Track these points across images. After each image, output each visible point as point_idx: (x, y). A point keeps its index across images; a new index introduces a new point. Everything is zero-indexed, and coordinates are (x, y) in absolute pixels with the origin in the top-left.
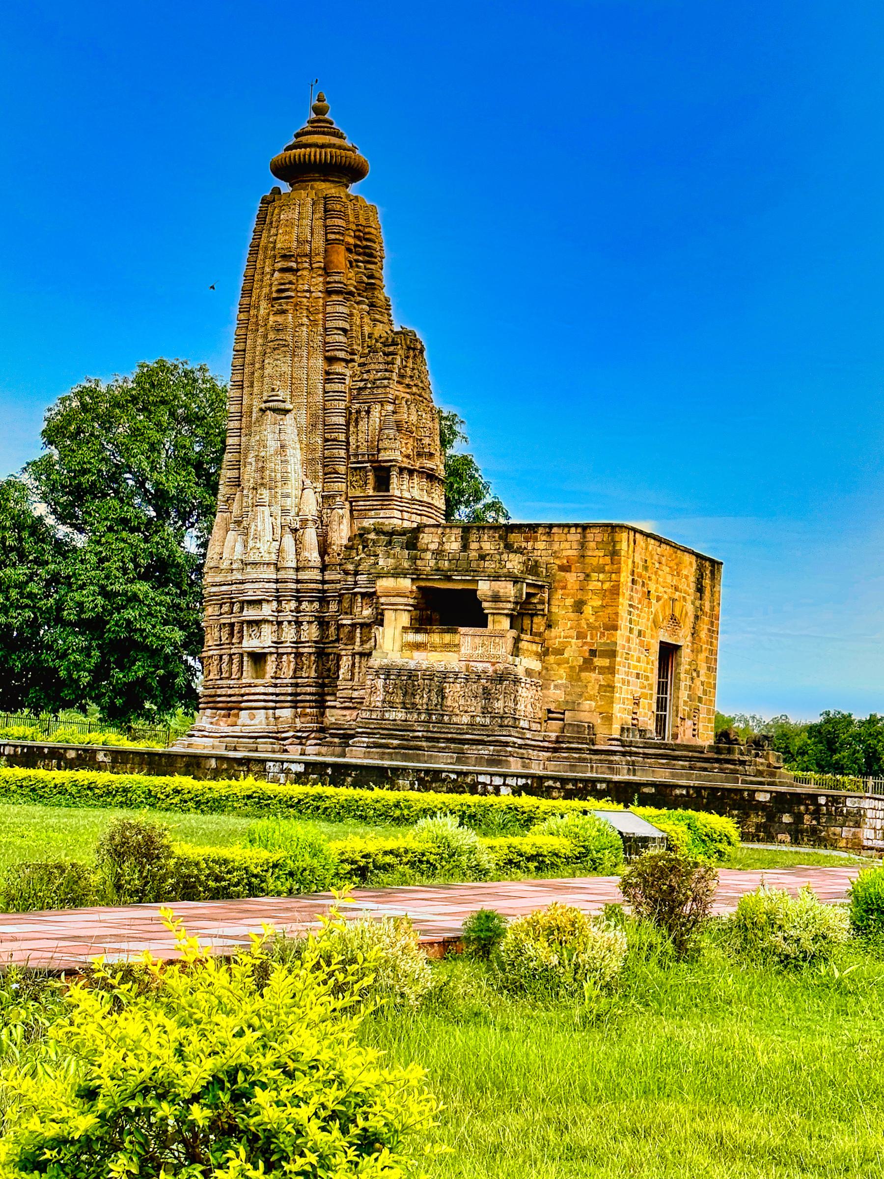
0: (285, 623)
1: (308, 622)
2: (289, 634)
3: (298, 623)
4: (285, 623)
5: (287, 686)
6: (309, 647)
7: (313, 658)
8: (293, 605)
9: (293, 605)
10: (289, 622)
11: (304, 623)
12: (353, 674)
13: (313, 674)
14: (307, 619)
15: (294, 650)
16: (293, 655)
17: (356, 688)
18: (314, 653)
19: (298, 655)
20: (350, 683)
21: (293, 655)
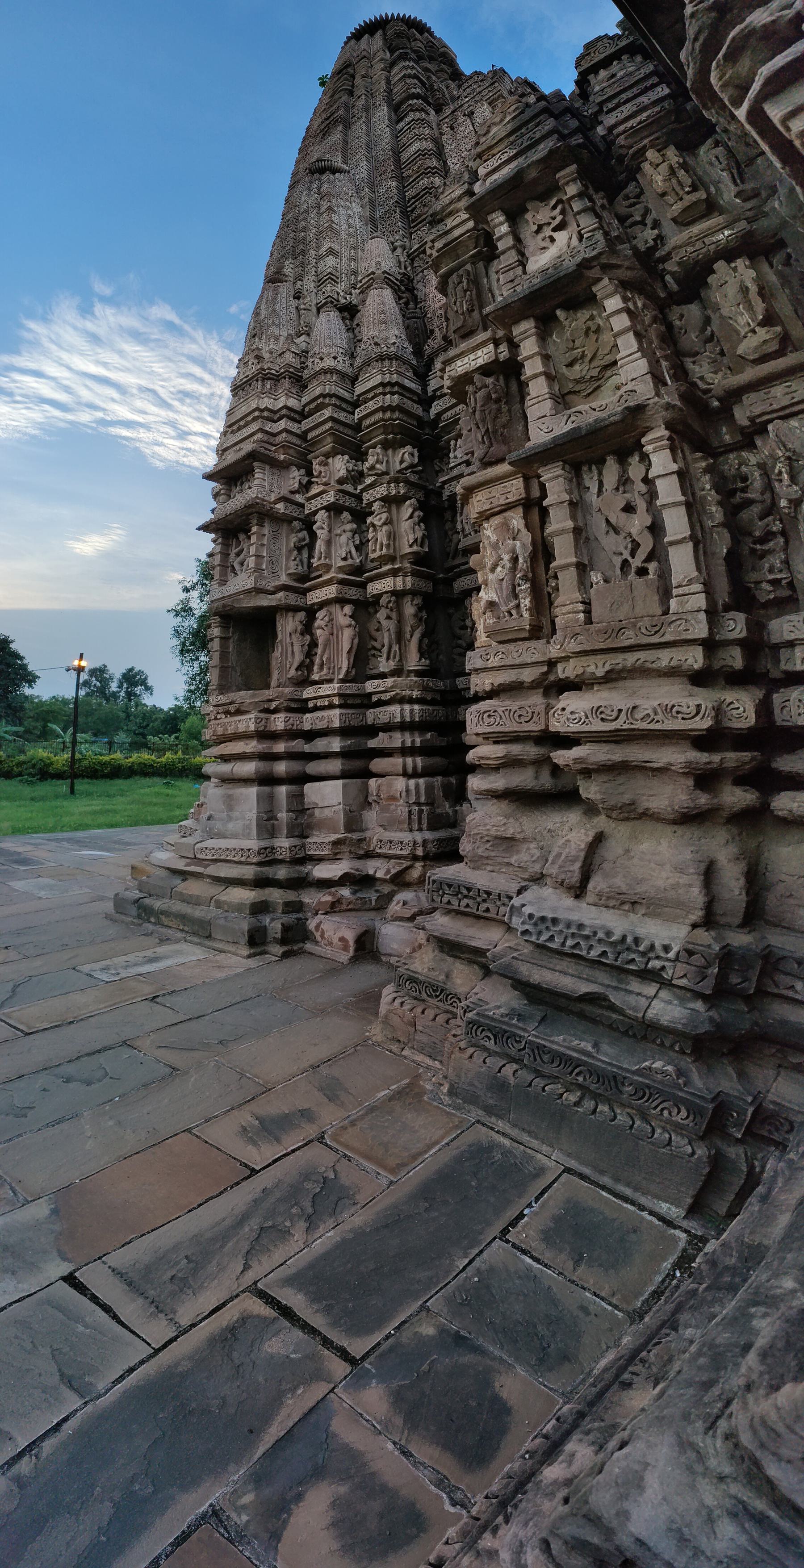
0: (322, 516)
1: (387, 500)
2: (336, 547)
3: (360, 516)
4: (322, 516)
5: (331, 706)
6: (394, 573)
7: (409, 609)
8: (340, 465)
9: (340, 465)
10: (334, 509)
11: (376, 506)
12: (543, 601)
13: (413, 661)
14: (381, 491)
15: (353, 593)
16: (348, 609)
17: (567, 671)
18: (413, 593)
19: (364, 608)
20: (535, 651)
21: (348, 609)
